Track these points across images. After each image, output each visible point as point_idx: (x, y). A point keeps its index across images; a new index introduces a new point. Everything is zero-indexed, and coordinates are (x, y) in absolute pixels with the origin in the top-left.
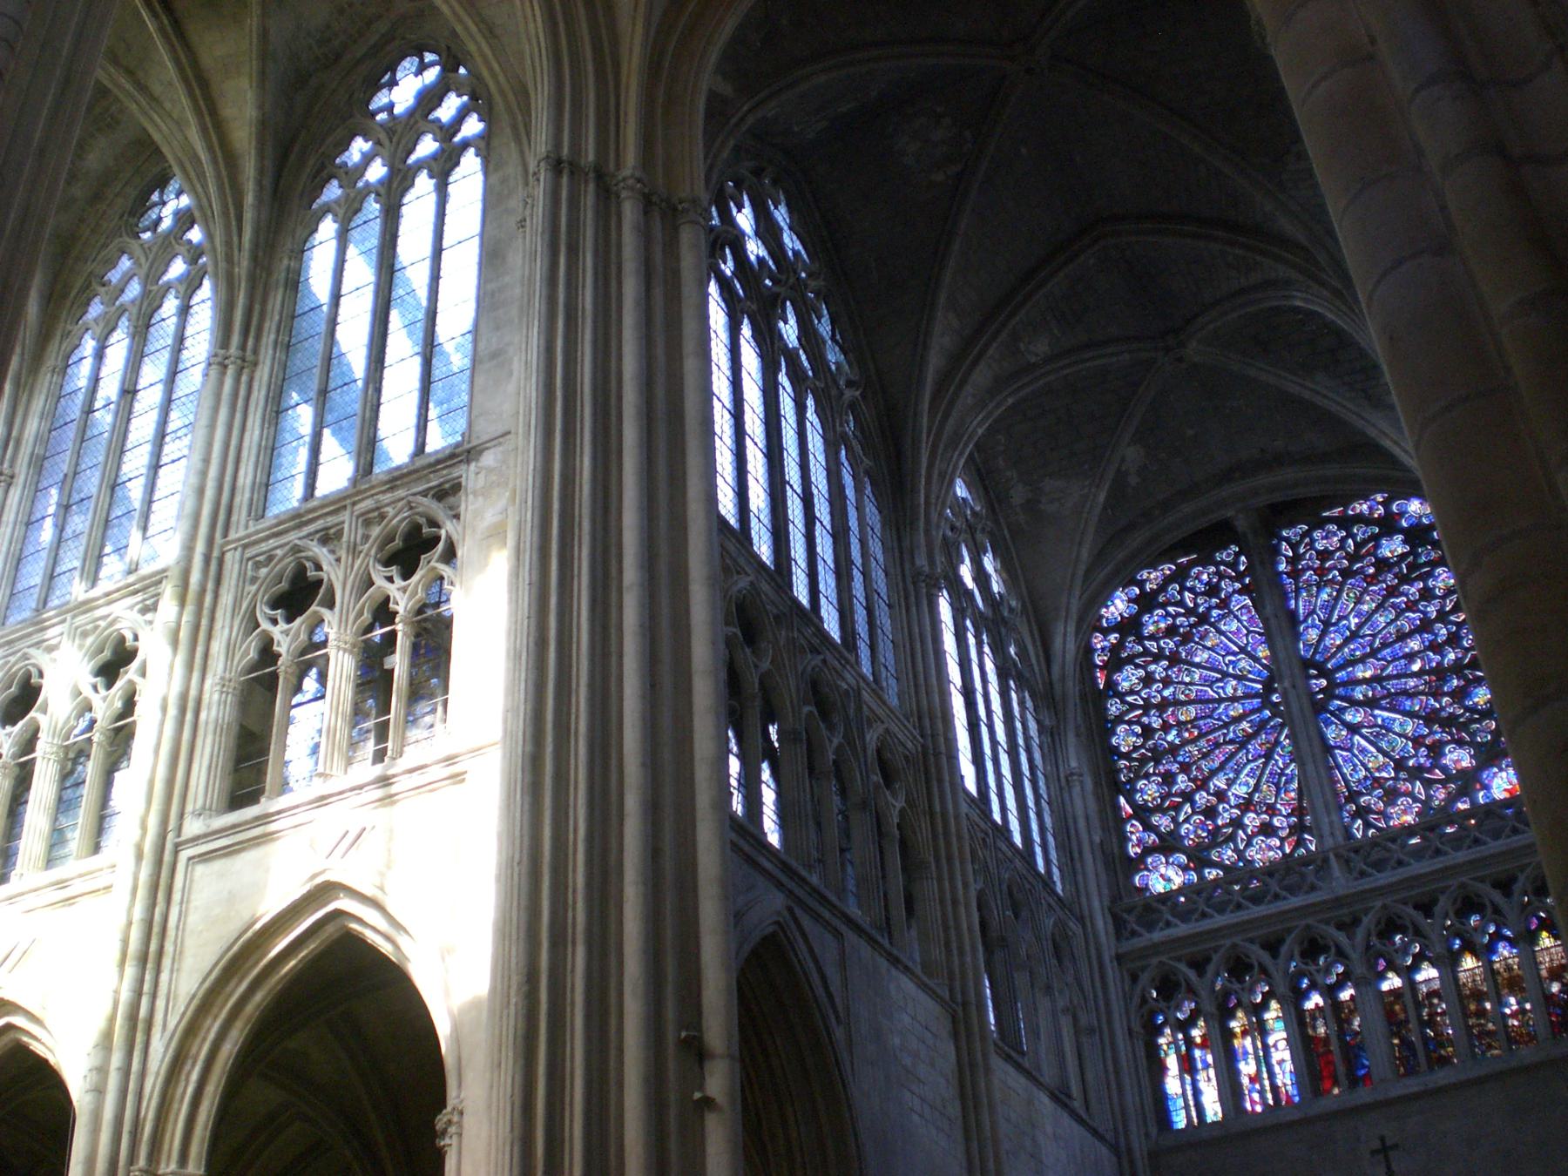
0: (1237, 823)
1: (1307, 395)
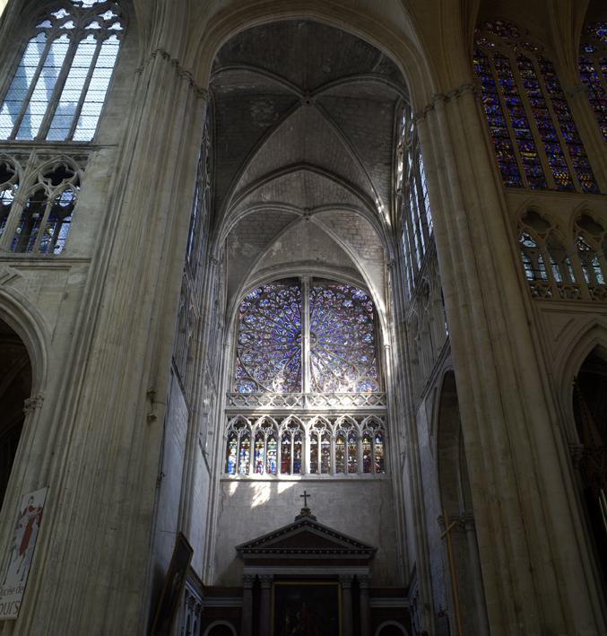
1: (341, 246)
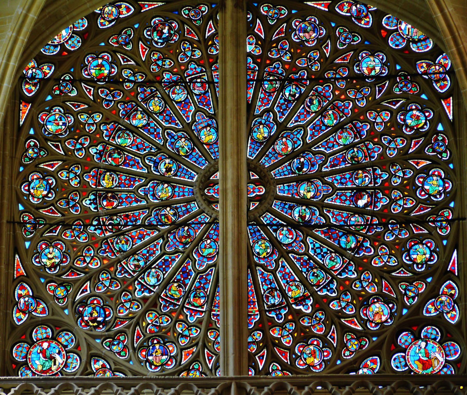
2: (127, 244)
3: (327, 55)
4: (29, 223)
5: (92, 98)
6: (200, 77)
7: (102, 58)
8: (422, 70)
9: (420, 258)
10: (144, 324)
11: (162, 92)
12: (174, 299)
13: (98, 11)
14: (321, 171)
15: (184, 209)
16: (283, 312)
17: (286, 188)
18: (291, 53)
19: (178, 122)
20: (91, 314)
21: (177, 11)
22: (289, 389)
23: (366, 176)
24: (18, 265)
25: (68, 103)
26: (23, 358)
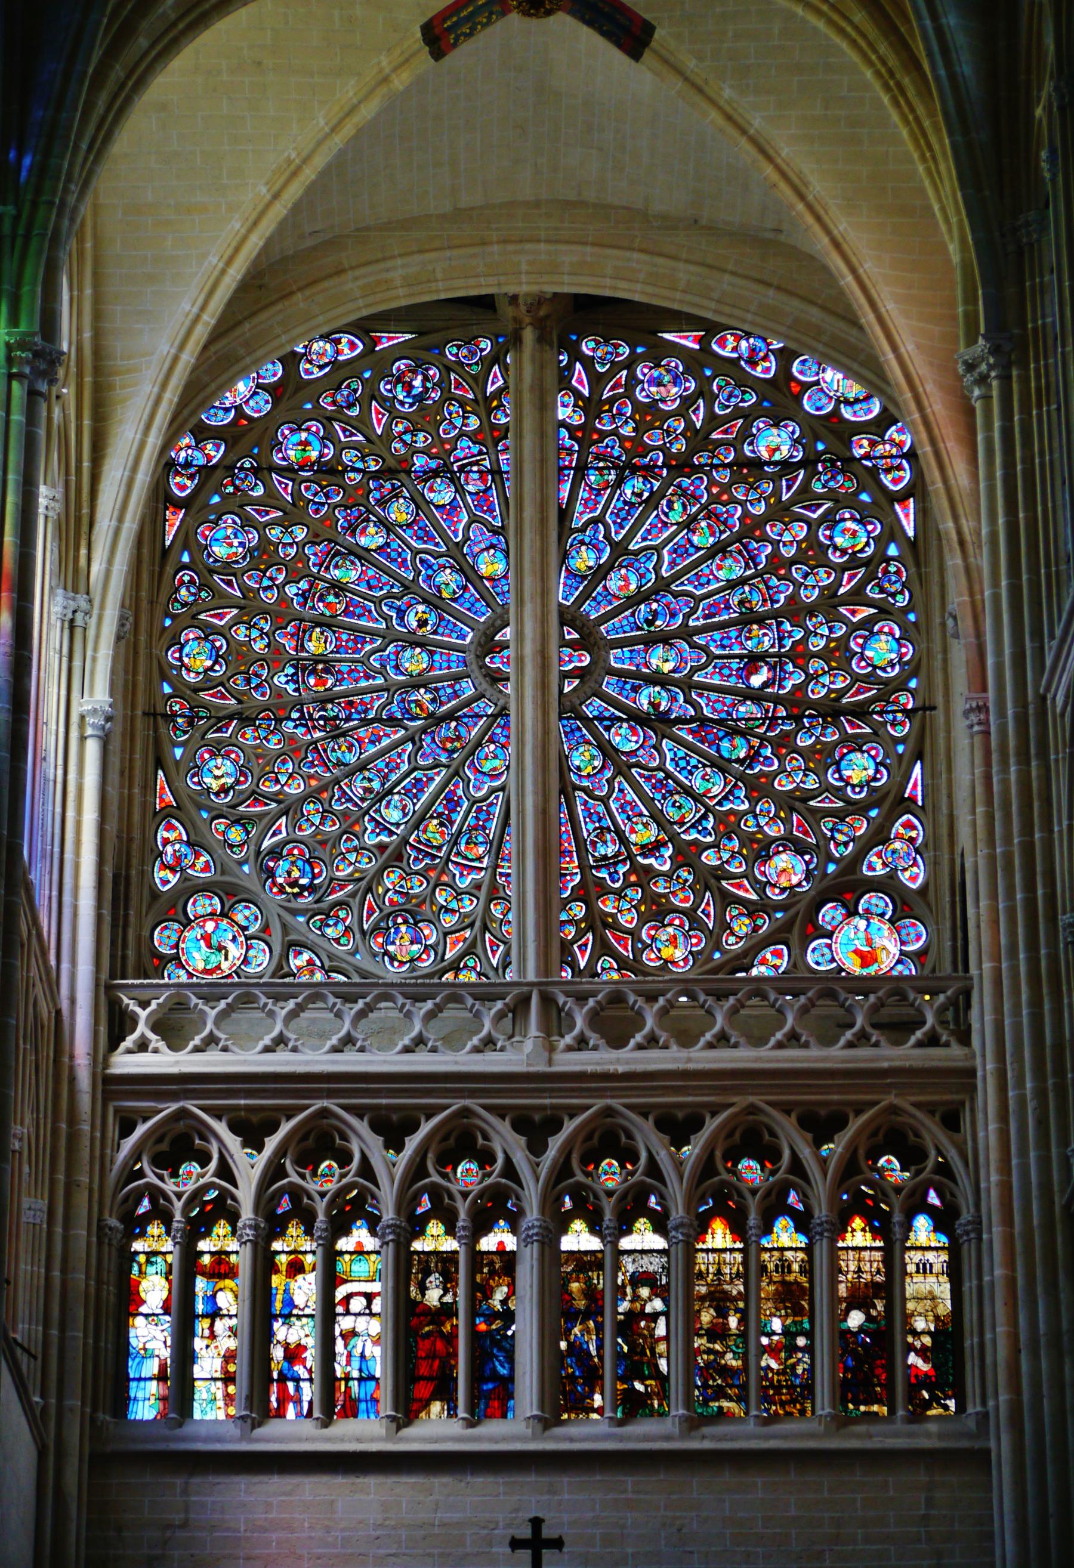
0: (370, 884)
2: (350, 751)
3: (698, 425)
4: (181, 716)
5: (289, 498)
6: (477, 463)
7: (308, 429)
8: (862, 451)
9: (857, 776)
10: (380, 890)
11: (411, 488)
12: (432, 847)
13: (300, 349)
14: (687, 625)
15: (449, 691)
16: (622, 869)
17: (627, 655)
18: (634, 421)
19: (438, 540)
20: (289, 873)
21: (437, 348)
22: (631, 1002)
23: (765, 635)
24: (162, 788)
25: (248, 508)
26: (172, 948)
